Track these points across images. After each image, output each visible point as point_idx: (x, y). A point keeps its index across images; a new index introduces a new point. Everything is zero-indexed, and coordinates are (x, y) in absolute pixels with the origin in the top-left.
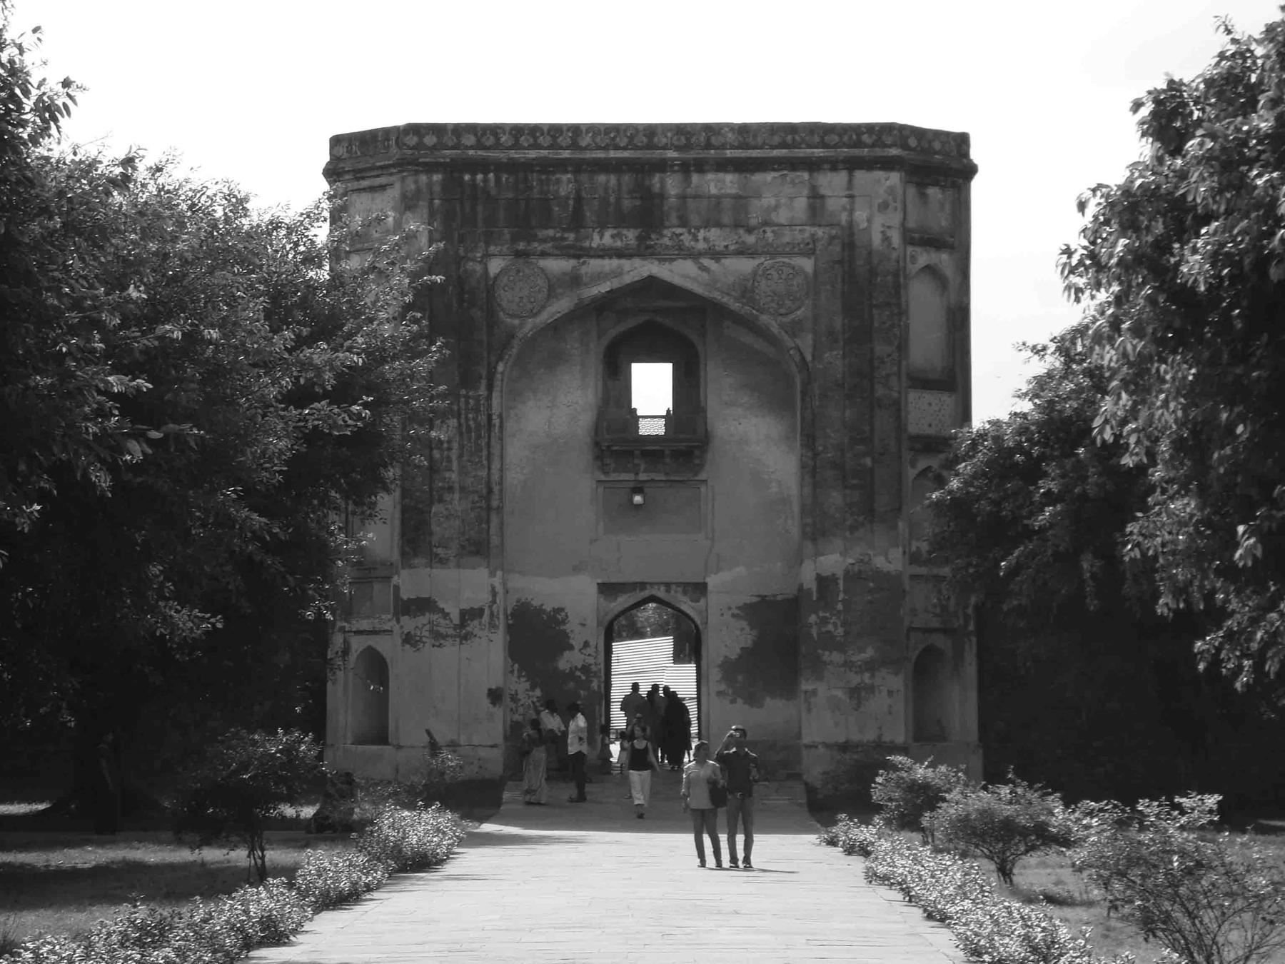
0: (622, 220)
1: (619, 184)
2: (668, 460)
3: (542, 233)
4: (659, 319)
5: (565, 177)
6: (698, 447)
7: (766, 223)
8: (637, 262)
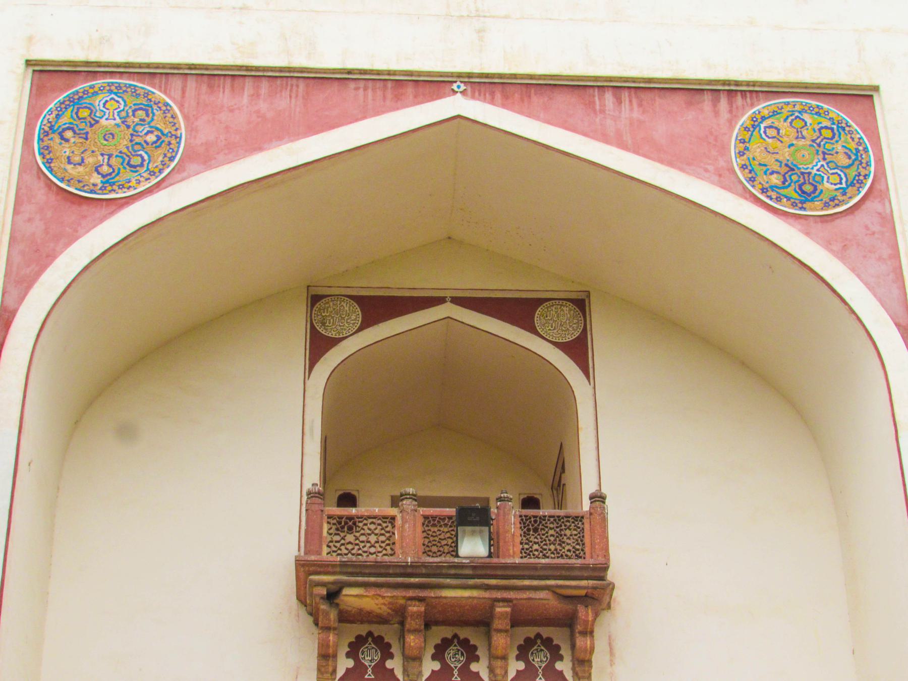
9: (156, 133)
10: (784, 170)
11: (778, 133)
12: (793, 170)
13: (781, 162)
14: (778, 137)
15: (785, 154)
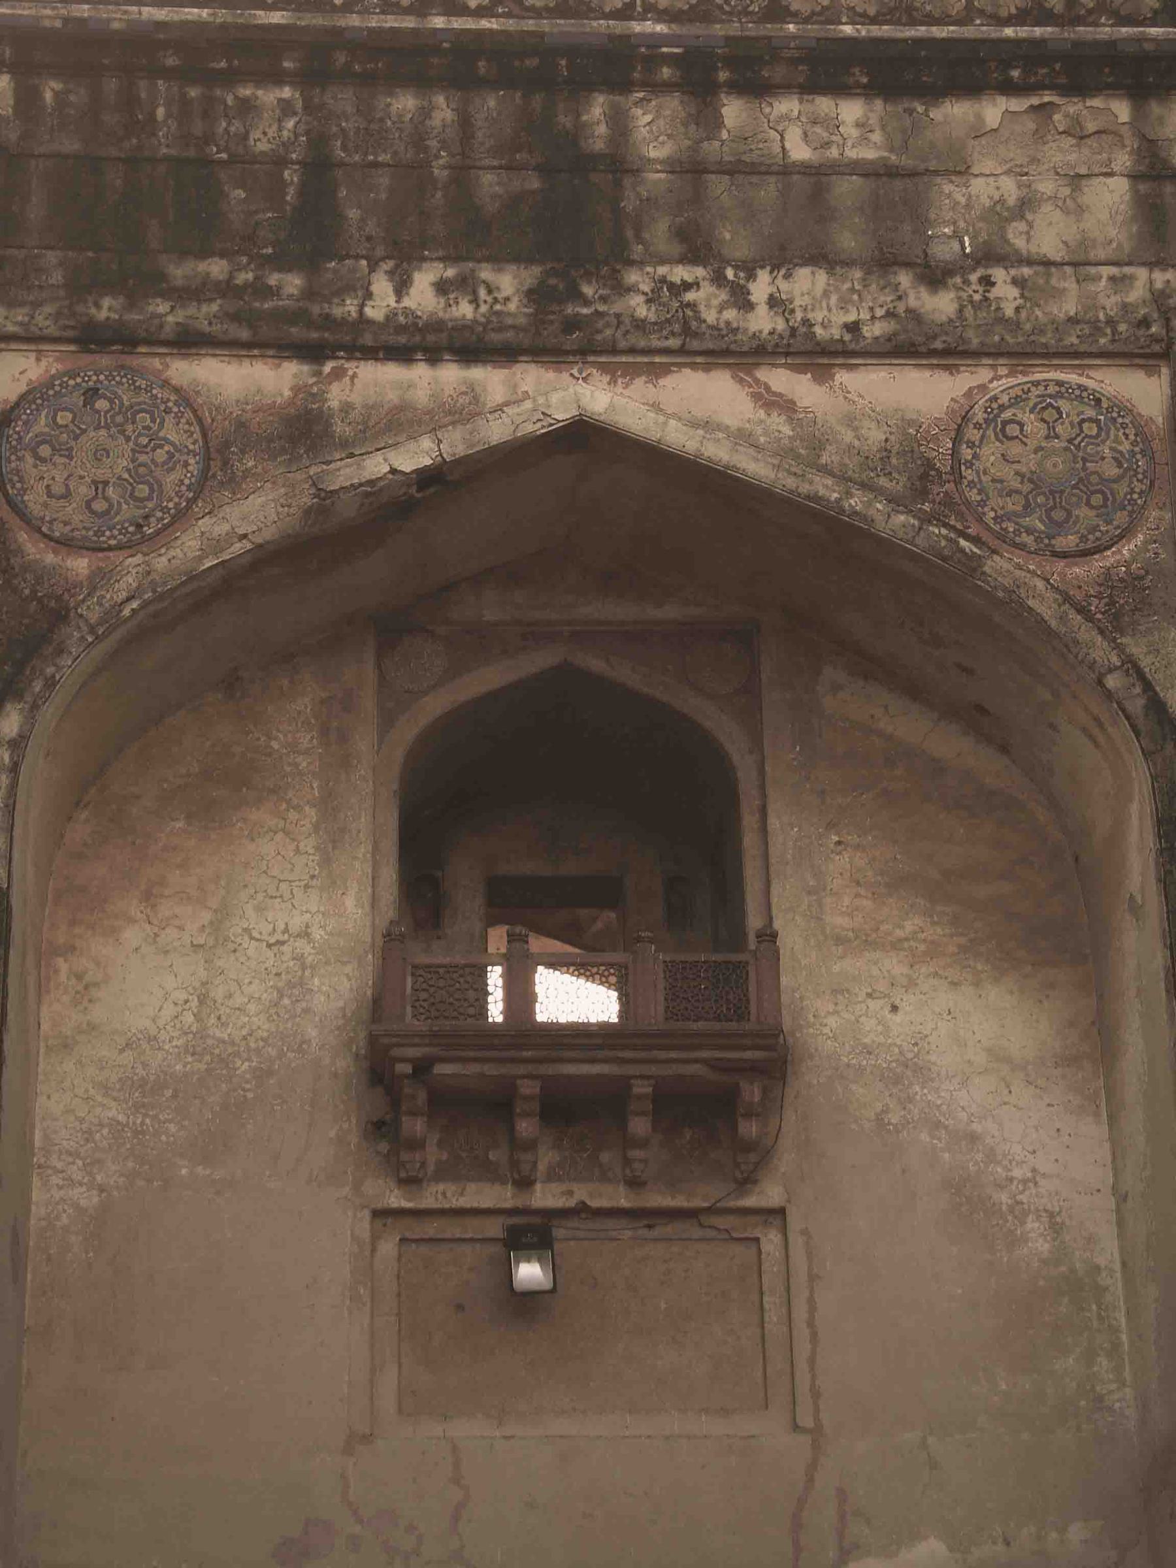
0: (472, 238)
1: (465, 122)
2: (639, 1126)
3: (180, 272)
4: (595, 664)
5: (269, 96)
6: (754, 1070)
7: (991, 254)
8: (530, 377)
9: (166, 448)
10: (1027, 487)
11: (1022, 430)
12: (1037, 487)
13: (1023, 476)
14: (1021, 439)
15: (1030, 463)
